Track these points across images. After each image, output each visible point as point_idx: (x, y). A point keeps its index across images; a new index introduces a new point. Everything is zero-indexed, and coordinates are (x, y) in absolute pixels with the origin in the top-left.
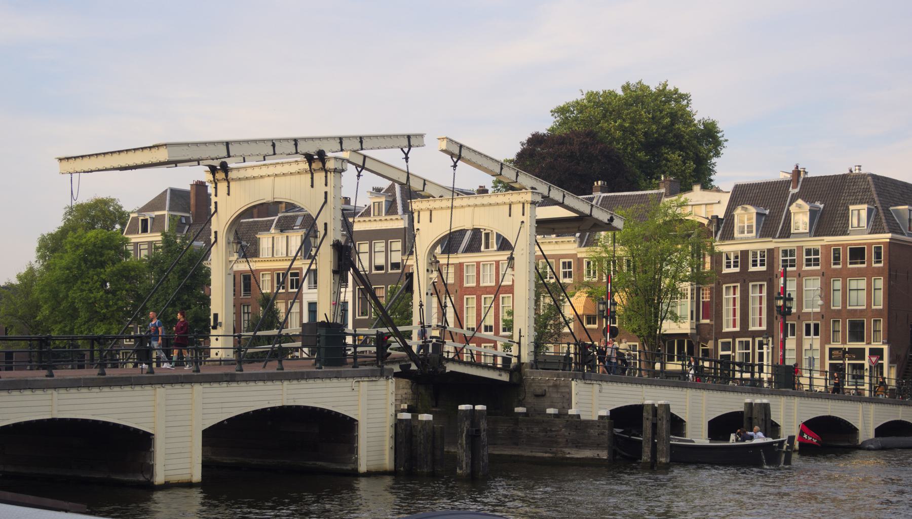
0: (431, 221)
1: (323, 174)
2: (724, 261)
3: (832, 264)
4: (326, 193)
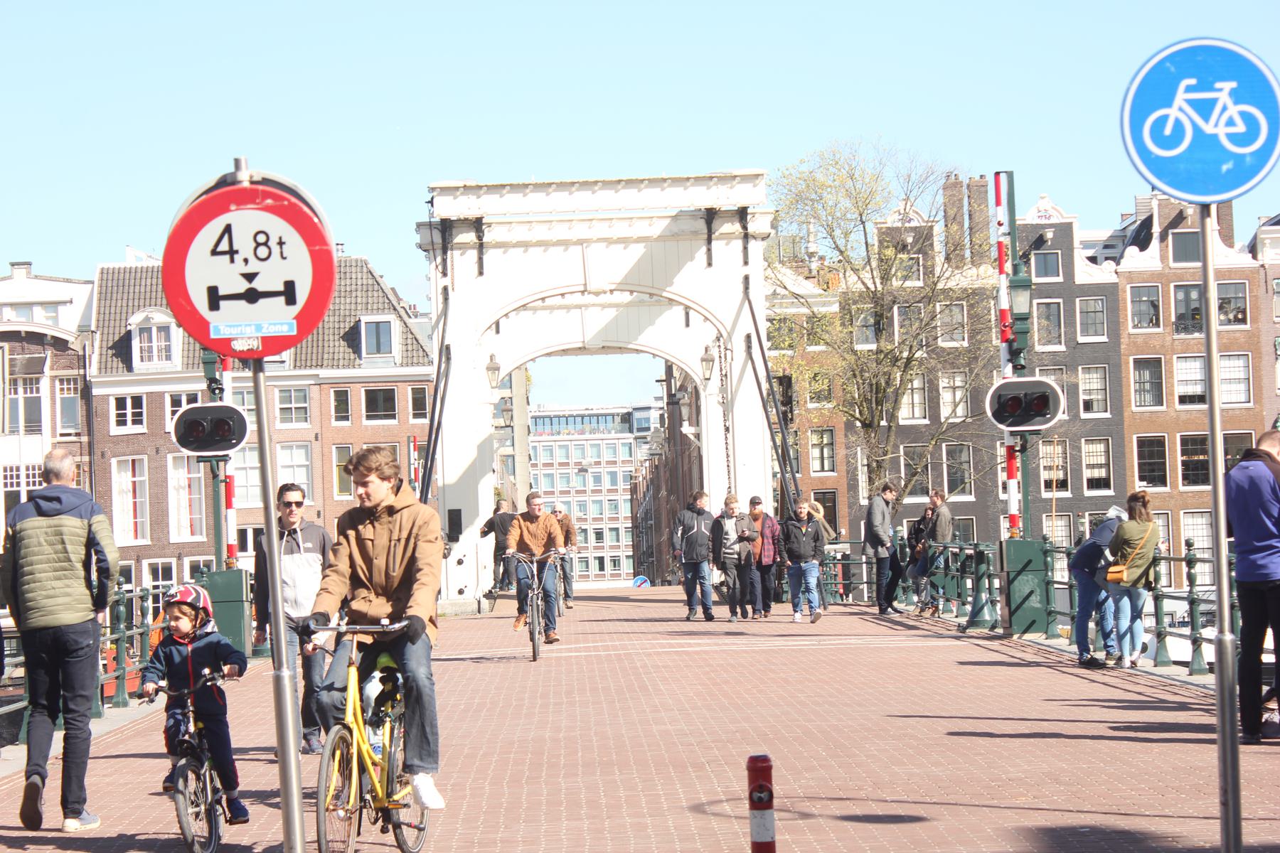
1: (738, 244)
3: (364, 418)
4: (746, 278)
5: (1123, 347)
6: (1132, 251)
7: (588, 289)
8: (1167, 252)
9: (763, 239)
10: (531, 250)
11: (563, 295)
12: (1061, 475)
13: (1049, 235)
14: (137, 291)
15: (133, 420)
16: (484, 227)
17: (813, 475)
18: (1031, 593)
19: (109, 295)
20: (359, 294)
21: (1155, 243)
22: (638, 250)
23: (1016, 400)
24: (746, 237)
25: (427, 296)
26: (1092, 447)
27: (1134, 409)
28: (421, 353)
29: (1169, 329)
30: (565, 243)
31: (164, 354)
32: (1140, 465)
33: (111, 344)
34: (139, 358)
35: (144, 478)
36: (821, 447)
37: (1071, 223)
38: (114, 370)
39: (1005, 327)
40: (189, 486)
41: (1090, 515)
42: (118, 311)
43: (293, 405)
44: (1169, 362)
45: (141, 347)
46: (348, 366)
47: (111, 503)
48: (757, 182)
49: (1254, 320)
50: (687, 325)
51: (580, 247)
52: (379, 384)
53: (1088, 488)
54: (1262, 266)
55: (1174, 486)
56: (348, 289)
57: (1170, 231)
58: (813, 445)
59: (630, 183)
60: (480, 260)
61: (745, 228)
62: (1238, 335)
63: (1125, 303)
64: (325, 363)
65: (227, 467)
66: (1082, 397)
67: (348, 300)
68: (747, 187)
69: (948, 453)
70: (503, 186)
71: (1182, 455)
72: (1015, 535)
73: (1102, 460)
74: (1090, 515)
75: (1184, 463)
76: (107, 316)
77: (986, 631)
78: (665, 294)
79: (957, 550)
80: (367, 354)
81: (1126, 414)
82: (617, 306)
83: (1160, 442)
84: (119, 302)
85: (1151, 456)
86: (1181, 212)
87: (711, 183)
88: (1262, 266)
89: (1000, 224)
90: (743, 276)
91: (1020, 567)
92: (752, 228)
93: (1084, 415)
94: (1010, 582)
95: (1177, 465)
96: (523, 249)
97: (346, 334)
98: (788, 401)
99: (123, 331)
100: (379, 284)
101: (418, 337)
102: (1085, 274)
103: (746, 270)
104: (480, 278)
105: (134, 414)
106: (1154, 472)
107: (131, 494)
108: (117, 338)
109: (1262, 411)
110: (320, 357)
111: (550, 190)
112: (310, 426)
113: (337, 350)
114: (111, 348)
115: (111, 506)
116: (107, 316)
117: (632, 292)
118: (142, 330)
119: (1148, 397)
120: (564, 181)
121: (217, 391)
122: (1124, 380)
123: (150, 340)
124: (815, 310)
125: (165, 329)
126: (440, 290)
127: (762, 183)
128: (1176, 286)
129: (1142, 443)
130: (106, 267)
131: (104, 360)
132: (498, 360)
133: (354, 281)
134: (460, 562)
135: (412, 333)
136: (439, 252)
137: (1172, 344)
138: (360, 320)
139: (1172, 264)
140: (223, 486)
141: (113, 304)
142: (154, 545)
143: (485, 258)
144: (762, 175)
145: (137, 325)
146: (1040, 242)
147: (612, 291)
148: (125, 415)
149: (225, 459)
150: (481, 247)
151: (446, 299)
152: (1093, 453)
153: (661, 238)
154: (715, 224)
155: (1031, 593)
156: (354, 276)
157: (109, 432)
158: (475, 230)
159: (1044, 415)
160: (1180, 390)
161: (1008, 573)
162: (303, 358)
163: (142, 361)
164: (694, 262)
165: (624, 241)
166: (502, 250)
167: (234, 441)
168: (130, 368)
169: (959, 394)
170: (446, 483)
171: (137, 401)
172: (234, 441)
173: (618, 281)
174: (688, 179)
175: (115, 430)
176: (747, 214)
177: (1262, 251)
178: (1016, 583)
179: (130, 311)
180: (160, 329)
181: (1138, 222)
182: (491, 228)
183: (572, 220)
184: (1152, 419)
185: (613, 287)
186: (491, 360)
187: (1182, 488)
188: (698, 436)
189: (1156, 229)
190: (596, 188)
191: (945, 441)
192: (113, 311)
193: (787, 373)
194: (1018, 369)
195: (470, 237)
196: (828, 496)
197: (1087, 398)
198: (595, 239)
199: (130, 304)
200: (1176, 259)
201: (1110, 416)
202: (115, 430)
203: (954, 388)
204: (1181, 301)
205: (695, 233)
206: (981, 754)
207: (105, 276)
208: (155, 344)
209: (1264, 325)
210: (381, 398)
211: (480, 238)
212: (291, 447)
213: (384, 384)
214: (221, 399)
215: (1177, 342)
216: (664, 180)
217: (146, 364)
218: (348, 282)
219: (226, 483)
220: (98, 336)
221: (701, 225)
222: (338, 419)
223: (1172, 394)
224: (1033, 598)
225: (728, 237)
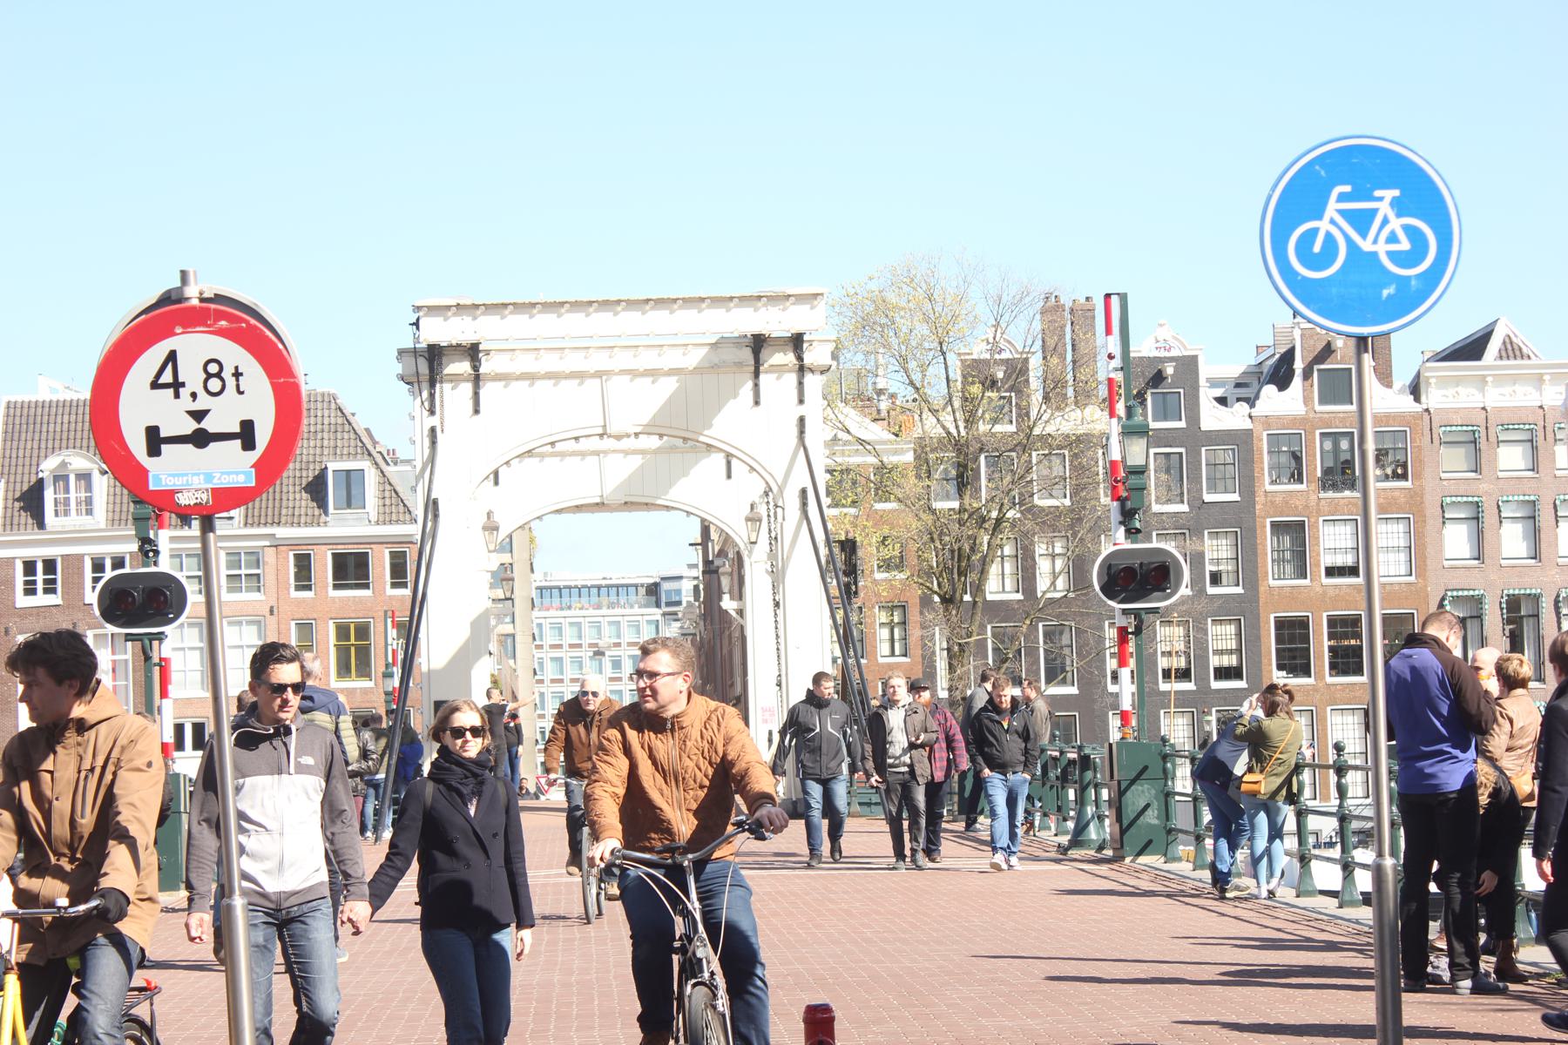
2: (20, 578)
3: (330, 588)
4: (802, 420)
5: (1257, 507)
6: (1270, 390)
7: (608, 432)
8: (1312, 392)
9: (822, 373)
10: (539, 383)
11: (577, 439)
12: (1183, 664)
13: (1170, 370)
14: (51, 429)
15: (44, 589)
16: (480, 355)
17: (881, 660)
18: (1147, 806)
19: (16, 435)
20: (326, 435)
21: (1297, 381)
22: (669, 385)
23: (1129, 570)
24: (802, 370)
25: (410, 439)
26: (1219, 629)
27: (1272, 583)
28: (401, 508)
29: (1314, 486)
30: (580, 376)
31: (84, 507)
32: (1278, 650)
33: (18, 494)
34: (53, 513)
36: (891, 626)
37: (1196, 356)
38: (22, 527)
39: (1116, 481)
40: (114, 670)
41: (1217, 711)
42: (28, 454)
43: (243, 571)
44: (1315, 526)
45: (56, 499)
46: (312, 524)
48: (816, 303)
49: (1417, 476)
50: (729, 476)
51: (598, 380)
52: (350, 546)
53: (1216, 678)
54: (1427, 410)
55: (1320, 677)
56: (312, 429)
57: (1316, 367)
58: (882, 624)
59: (661, 303)
60: (476, 395)
61: (800, 358)
62: (1397, 494)
63: (1261, 454)
64: (283, 519)
65: (163, 646)
66: (1209, 568)
67: (312, 443)
68: (804, 309)
69: (1046, 635)
70: (505, 305)
71: (1329, 639)
72: (1128, 736)
74: (1217, 711)
75: (1331, 649)
76: (14, 460)
77: (1092, 852)
78: (702, 439)
79: (1057, 754)
80: (335, 509)
81: (1262, 589)
82: (642, 452)
83: (1303, 624)
84: (29, 443)
85: (1292, 640)
86: (1329, 344)
87: (760, 304)
88: (1427, 410)
89: (1111, 357)
90: (798, 417)
91: (1134, 774)
92: (809, 359)
93: (1211, 590)
94: (1121, 793)
95: (1323, 651)
96: (528, 382)
97: (309, 484)
98: (852, 570)
99: (34, 480)
100: (350, 424)
101: (398, 489)
102: (1213, 418)
103: (801, 410)
104: (476, 417)
105: (46, 582)
106: (1295, 660)
108: (25, 487)
109: (1426, 586)
110: (276, 513)
111: (563, 310)
112: (263, 598)
113: (297, 503)
114: (18, 500)
116: (14, 460)
117: (661, 436)
118: (56, 478)
119: (1289, 568)
120: (579, 299)
121: (151, 554)
122: (1260, 547)
123: (67, 490)
124: (885, 460)
125: (85, 477)
126: (426, 432)
127: (821, 305)
128: (1321, 434)
129: (1281, 624)
130: (13, 400)
131: (9, 514)
132: (496, 518)
133: (319, 419)
135: (390, 484)
136: (425, 386)
137: (1318, 504)
138: (326, 468)
139: (1318, 408)
140: (157, 670)
141: (22, 446)
143: (482, 392)
144: (822, 294)
145: (51, 472)
146: (1158, 379)
147: (636, 435)
148: (34, 582)
149: (160, 637)
150: (477, 379)
151: (433, 443)
152: (1222, 636)
153: (698, 370)
154: (764, 354)
155: (1147, 806)
156: (319, 414)
157: (15, 603)
158: (469, 358)
159: (1164, 590)
160: (1328, 560)
161: (1119, 782)
162: (256, 514)
163: (57, 515)
164: (739, 399)
165: (653, 373)
166: (503, 383)
167: (172, 616)
168: (41, 524)
169: (1059, 563)
171: (50, 566)
172: (172, 616)
173: (645, 423)
174: (731, 298)
175: (22, 601)
176: (802, 341)
177: (1427, 392)
178: (1129, 794)
179: (42, 454)
180: (80, 476)
181: (1277, 356)
182: (489, 357)
183: (589, 348)
184: (1293, 595)
185: (638, 429)
186: (489, 518)
187: (1330, 680)
188: (741, 612)
189: (1299, 365)
190: (619, 309)
191: (1042, 620)
192: (21, 454)
193: (851, 536)
194: (1132, 533)
195: (462, 367)
197: (1214, 568)
198: (617, 371)
199: (43, 446)
200: (1322, 401)
201: (1242, 592)
202: (22, 601)
203: (1053, 556)
204: (1328, 452)
205: (739, 364)
206: (1087, 1004)
207: (12, 411)
208: (73, 495)
209: (1429, 483)
210: (351, 562)
211: (476, 368)
212: (240, 623)
213: (356, 546)
214: (156, 564)
215: (1323, 502)
216: (702, 300)
217: (62, 520)
218: (312, 420)
219: (161, 666)
221: (747, 355)
222: (298, 588)
223: (1318, 565)
224: (1149, 812)
225: (779, 369)
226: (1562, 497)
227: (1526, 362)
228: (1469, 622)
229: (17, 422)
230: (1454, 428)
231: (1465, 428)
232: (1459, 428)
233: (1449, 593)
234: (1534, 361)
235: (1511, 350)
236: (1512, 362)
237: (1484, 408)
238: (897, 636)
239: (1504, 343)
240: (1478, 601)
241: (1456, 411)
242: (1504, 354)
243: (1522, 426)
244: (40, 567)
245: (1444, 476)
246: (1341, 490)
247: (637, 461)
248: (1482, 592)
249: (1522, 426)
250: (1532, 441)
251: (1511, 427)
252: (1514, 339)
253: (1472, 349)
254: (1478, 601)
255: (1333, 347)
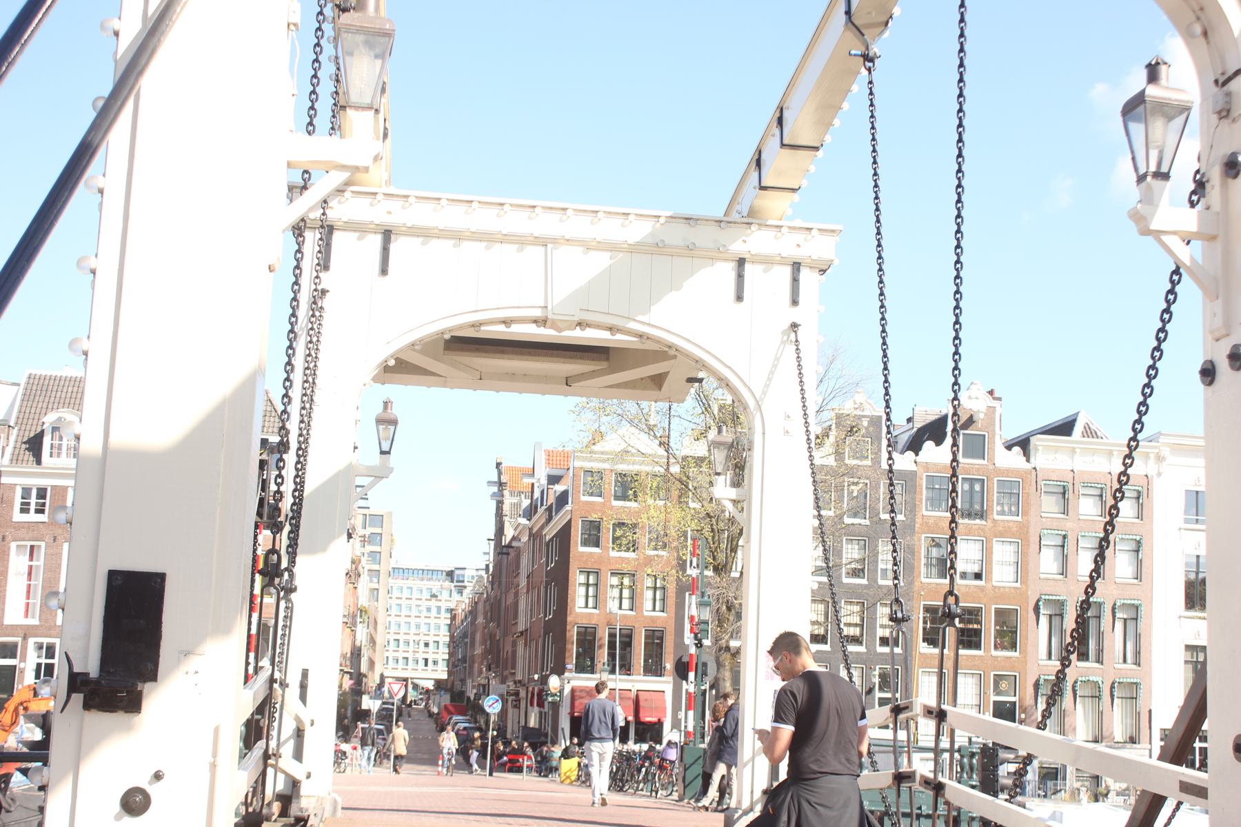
0: (384, 271)
2: (18, 501)
5: (917, 526)
6: (929, 445)
12: (822, 632)
14: (58, 396)
17: (646, 614)
19: (32, 397)
21: (949, 440)
27: (924, 580)
31: (72, 452)
33: (25, 439)
35: (39, 562)
41: (880, 668)
42: (38, 412)
45: (52, 444)
47: (6, 583)
49: (1025, 513)
50: (739, 298)
53: (880, 645)
54: (1035, 468)
62: (1011, 524)
63: (921, 489)
73: (857, 620)
74: (880, 668)
76: (27, 415)
82: (611, 247)
86: (971, 416)
99: (39, 430)
107: (26, 576)
108: (32, 435)
109: (1027, 591)
114: (25, 443)
115: (6, 586)
118: (55, 429)
119: (934, 571)
122: (916, 554)
128: (963, 478)
130: (34, 373)
131: (17, 452)
134: (134, 803)
141: (34, 405)
142: (42, 626)
148: (28, 504)
157: (12, 518)
163: (51, 456)
168: (39, 462)
170: (116, 440)
171: (42, 493)
175: (18, 517)
181: (915, 430)
192: (33, 411)
196: (656, 634)
202: (18, 517)
204: (966, 491)
207: (31, 381)
220: (15, 432)
226: (1120, 536)
227: (1099, 440)
228: (1053, 618)
229: (34, 388)
230: (1051, 482)
231: (1059, 483)
232: (1055, 483)
233: (1043, 597)
234: (1105, 440)
235: (1089, 432)
236: (1090, 440)
237: (1072, 471)
238: (658, 597)
239: (1085, 427)
240: (1061, 604)
241: (1054, 471)
242: (1085, 435)
243: (1096, 485)
244: (34, 493)
245: (1043, 515)
246: (975, 519)
247: (602, 260)
248: (1065, 598)
249: (1096, 485)
250: (1101, 496)
251: (1089, 485)
252: (1091, 426)
253: (1064, 428)
254: (1061, 604)
255: (974, 419)
